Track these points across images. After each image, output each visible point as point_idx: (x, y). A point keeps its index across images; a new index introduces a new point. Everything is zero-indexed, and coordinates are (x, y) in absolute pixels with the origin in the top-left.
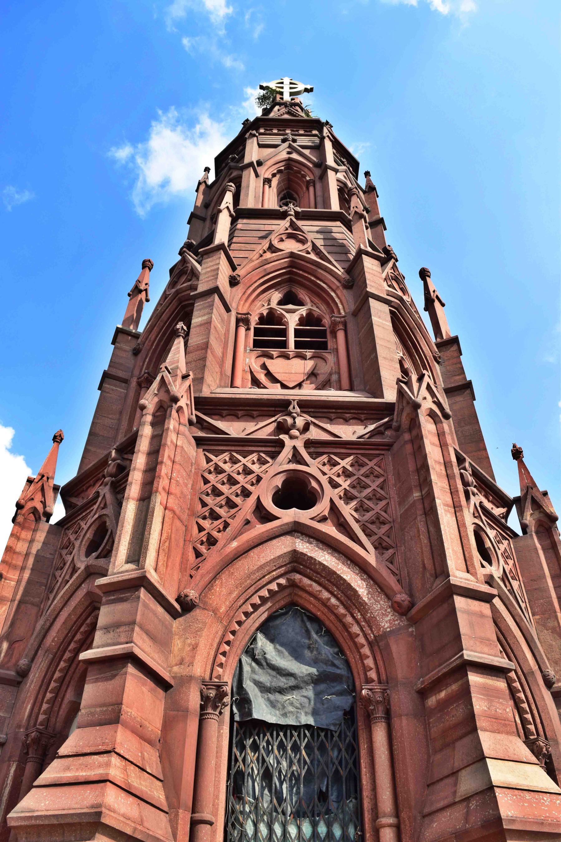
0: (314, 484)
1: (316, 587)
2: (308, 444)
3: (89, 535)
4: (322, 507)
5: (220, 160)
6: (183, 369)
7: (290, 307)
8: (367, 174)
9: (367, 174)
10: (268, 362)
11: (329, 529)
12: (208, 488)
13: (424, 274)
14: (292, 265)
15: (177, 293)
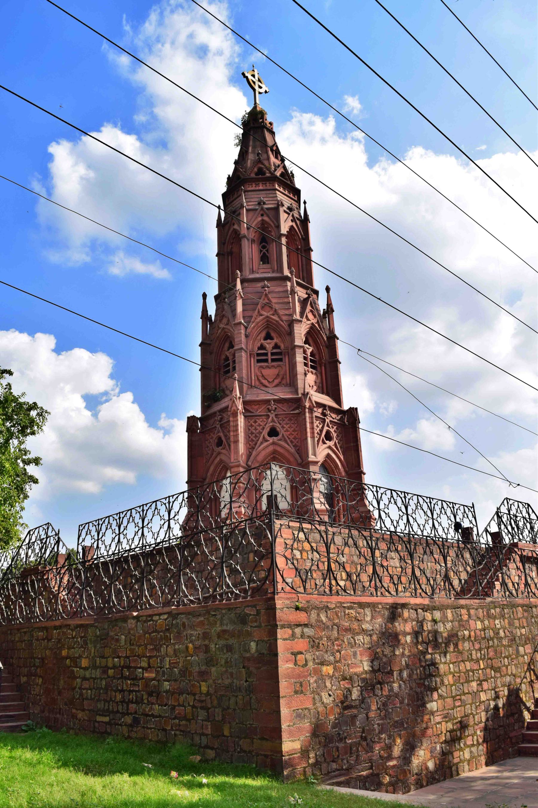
0: (278, 429)
1: (279, 457)
2: (276, 415)
3: (216, 441)
4: (280, 436)
5: (224, 196)
6: (238, 395)
7: (269, 341)
8: (305, 203)
9: (305, 203)
10: (263, 371)
11: (282, 443)
12: (250, 432)
13: (328, 289)
14: (268, 321)
15: (224, 328)
